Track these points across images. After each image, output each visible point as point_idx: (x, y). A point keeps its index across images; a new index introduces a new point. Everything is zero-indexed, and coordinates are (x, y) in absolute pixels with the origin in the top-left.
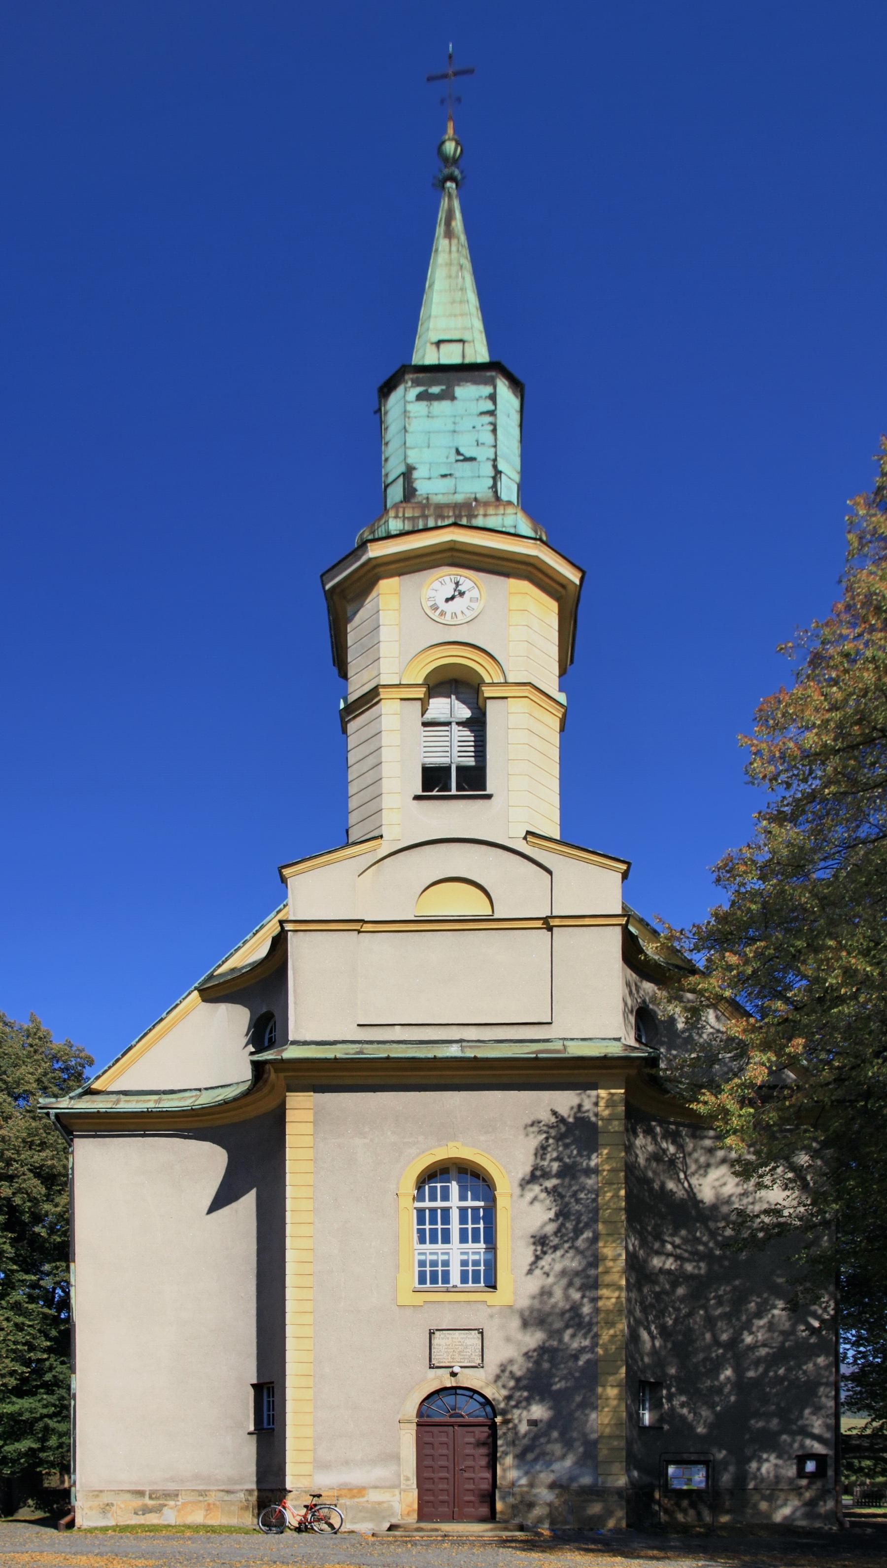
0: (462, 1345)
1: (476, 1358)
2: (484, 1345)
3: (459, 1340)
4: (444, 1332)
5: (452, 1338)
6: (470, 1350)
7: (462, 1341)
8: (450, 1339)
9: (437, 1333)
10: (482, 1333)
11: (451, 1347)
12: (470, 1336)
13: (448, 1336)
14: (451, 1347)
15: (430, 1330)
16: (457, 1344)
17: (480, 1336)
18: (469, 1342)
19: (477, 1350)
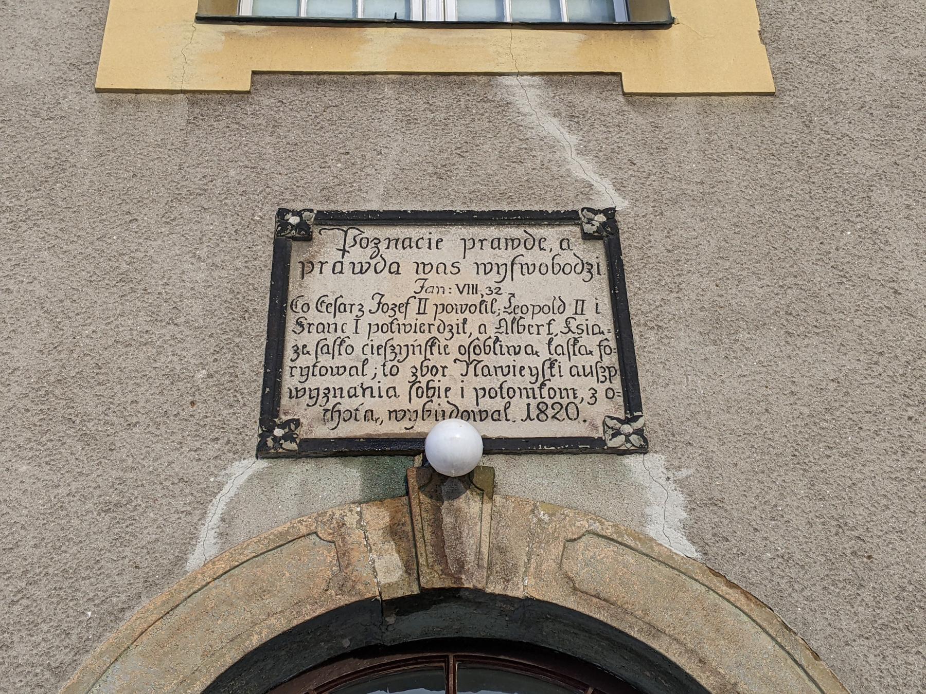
2: (634, 305)
3: (469, 275)
5: (421, 267)
6: (539, 342)
7: (486, 282)
8: (408, 269)
11: (412, 316)
13: (391, 255)
14: (412, 316)
16: (455, 298)
19: (590, 341)
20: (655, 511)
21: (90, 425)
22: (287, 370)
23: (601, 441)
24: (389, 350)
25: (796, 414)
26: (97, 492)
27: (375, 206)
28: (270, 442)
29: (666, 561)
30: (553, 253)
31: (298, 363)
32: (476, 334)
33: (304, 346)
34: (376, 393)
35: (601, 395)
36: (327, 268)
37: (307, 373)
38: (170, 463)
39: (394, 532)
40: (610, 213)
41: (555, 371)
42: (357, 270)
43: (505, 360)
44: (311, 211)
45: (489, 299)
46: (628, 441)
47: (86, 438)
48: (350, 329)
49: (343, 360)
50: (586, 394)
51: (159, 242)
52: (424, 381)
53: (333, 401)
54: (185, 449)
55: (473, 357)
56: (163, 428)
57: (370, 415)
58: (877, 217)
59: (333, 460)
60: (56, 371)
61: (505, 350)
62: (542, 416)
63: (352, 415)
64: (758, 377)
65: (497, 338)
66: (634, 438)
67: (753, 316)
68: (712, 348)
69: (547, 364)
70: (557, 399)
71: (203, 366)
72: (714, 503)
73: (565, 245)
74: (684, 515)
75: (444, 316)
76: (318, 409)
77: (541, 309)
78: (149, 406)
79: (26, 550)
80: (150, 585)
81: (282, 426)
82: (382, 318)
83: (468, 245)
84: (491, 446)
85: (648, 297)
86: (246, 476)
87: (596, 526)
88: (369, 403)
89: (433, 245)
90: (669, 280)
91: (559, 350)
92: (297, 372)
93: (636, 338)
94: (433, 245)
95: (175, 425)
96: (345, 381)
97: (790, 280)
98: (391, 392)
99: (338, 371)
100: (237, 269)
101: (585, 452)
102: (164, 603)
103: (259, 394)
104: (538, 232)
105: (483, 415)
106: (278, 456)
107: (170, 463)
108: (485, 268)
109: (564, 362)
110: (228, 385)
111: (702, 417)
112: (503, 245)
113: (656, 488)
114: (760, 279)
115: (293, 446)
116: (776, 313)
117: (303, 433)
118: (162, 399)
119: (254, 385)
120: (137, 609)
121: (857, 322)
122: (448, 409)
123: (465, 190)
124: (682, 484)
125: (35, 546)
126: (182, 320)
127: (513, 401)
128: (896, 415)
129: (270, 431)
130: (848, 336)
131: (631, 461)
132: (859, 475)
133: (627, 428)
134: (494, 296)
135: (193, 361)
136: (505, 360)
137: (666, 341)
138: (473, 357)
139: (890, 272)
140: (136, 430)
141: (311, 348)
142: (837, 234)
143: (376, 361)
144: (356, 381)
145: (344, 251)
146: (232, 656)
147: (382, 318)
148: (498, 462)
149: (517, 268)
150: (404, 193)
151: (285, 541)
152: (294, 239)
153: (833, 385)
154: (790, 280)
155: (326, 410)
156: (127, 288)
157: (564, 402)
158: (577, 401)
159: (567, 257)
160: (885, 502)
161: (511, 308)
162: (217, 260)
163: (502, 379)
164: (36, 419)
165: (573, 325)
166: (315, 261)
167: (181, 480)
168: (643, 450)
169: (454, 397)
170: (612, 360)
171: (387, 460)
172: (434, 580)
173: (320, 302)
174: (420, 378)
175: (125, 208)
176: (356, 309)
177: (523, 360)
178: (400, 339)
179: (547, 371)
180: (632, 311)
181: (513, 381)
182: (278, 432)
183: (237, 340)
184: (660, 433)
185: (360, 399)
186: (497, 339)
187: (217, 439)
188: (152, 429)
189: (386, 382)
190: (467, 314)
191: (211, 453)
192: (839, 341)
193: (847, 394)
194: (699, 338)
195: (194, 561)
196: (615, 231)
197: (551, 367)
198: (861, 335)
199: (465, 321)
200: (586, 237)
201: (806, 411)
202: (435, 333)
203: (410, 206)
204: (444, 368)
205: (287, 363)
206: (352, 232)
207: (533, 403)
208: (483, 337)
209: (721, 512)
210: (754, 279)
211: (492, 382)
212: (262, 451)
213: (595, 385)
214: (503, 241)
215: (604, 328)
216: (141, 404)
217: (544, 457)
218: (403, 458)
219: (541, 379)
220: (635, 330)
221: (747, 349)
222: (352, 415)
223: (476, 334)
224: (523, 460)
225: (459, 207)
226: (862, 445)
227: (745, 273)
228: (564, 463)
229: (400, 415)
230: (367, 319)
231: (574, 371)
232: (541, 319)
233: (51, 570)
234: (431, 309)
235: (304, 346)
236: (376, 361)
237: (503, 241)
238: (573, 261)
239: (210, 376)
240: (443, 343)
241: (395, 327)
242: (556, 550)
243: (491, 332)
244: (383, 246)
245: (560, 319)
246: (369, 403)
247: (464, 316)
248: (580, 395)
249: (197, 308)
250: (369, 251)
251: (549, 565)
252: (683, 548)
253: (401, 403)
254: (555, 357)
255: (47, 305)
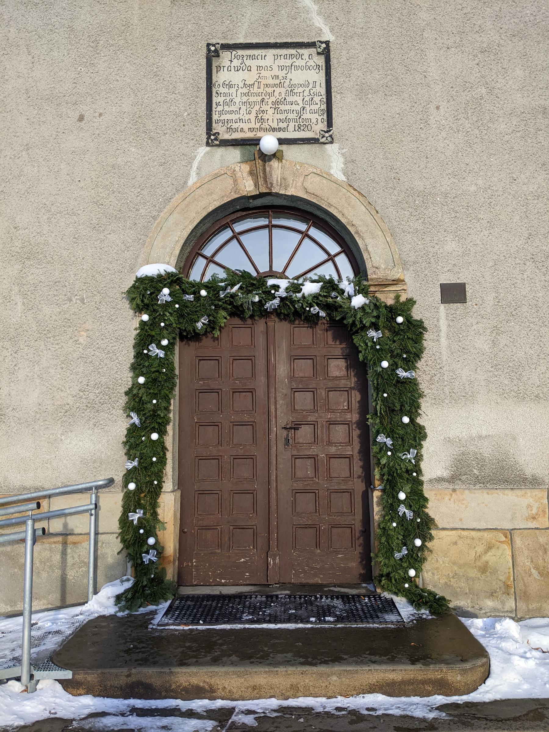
0: (280, 85)
1: (314, 117)
3: (276, 72)
4: (240, 52)
5: (259, 67)
6: (299, 99)
7: (282, 74)
8: (254, 69)
9: (226, 55)
10: (326, 53)
11: (255, 90)
12: (299, 62)
13: (248, 62)
14: (255, 90)
15: (208, 45)
16: (270, 81)
17: (321, 60)
18: (297, 77)
19: (317, 99)
20: (334, 165)
21: (152, 134)
22: (214, 112)
23: (318, 139)
24: (248, 104)
25: (384, 127)
26: (157, 159)
27: (241, 40)
28: (210, 141)
29: (336, 182)
30: (306, 61)
31: (217, 109)
32: (278, 97)
33: (219, 102)
34: (244, 121)
35: (319, 121)
36: (226, 69)
37: (221, 113)
38: (179, 148)
39: (251, 173)
40: (327, 43)
41: (305, 111)
42: (236, 69)
43: (287, 107)
44: (218, 44)
45: (282, 81)
46: (327, 139)
47: (151, 138)
48: (234, 95)
49: (233, 108)
50: (314, 121)
51: (166, 59)
52: (260, 116)
53: (230, 124)
54: (183, 143)
55: (277, 106)
56: (175, 135)
57: (242, 130)
58: (424, 44)
59: (231, 147)
60: (138, 113)
61: (288, 103)
62: (299, 130)
63: (236, 130)
64: (373, 113)
65: (285, 98)
66: (329, 138)
67: (374, 88)
68: (358, 101)
69: (302, 109)
70: (305, 123)
71: (186, 110)
72: (353, 161)
73: (310, 57)
74: (343, 166)
75: (267, 89)
76: (225, 128)
77: (301, 86)
78: (170, 127)
79: (138, 179)
80: (178, 191)
81: (214, 135)
82: (245, 90)
83: (276, 57)
84: (281, 141)
85: (339, 80)
86: (203, 153)
87: (315, 171)
88: (242, 125)
89: (263, 58)
90: (346, 72)
91: (306, 103)
92: (217, 113)
93: (333, 97)
94: (263, 58)
95: (179, 134)
96: (234, 117)
97: (389, 72)
98: (249, 121)
99: (231, 112)
100: (194, 70)
101: (313, 143)
102: (183, 197)
103: (205, 122)
104: (301, 51)
105: (280, 129)
106: (213, 146)
107: (179, 148)
108: (281, 68)
109: (308, 108)
110: (195, 118)
111: (352, 129)
112: (288, 57)
113: (335, 157)
114: (379, 72)
115: (218, 143)
116: (382, 86)
117: (220, 137)
118: (174, 124)
119: (203, 118)
120: (175, 198)
121: (410, 90)
122: (268, 127)
123: (275, 32)
124: (343, 154)
125: (141, 177)
126: (177, 92)
127: (290, 124)
128: (417, 127)
129: (210, 137)
130: (406, 95)
131: (328, 146)
132: (400, 150)
133: (327, 135)
134: (284, 80)
135: (182, 109)
136: (287, 107)
137: (343, 99)
138: (277, 106)
139: (424, 68)
140: (167, 136)
141: (221, 103)
142: (408, 51)
143: (244, 108)
144: (237, 116)
145: (231, 61)
146: (204, 214)
147: (245, 90)
148: (284, 147)
149: (293, 67)
150: (252, 34)
151: (217, 176)
152: (213, 56)
153: (398, 116)
154: (389, 72)
155: (228, 128)
156: (157, 78)
157: (307, 124)
158: (311, 124)
159: (311, 63)
160: (407, 160)
161: (291, 86)
162: (187, 66)
163: (286, 115)
164: (134, 131)
165: (312, 92)
166: (221, 66)
167: (183, 154)
168: (332, 142)
169: (270, 122)
170: (324, 107)
171: (248, 147)
172: (264, 190)
173: (224, 84)
174: (259, 115)
175: (153, 44)
176: (236, 86)
177: (294, 107)
178: (252, 99)
179: (302, 112)
180: (332, 86)
181: (291, 116)
182: (212, 137)
183: (196, 100)
184: (338, 135)
185: (239, 124)
186: (285, 98)
187: (193, 139)
188: (172, 135)
189: (247, 117)
190: (275, 88)
191: (192, 145)
192: (402, 97)
193: (402, 119)
194: (355, 97)
195: (190, 183)
196: (329, 51)
197: (303, 110)
198: (410, 95)
199: (274, 91)
200: (319, 54)
201: (387, 126)
202: (264, 97)
203: (255, 41)
204: (267, 111)
205: (214, 109)
206: (234, 53)
207: (297, 124)
208: (280, 98)
209: (355, 165)
210: (376, 71)
211: (282, 116)
212: (208, 144)
213: (318, 117)
214: (288, 55)
215: (322, 94)
216: (167, 126)
217: (299, 145)
218: (253, 146)
219: (299, 115)
220: (333, 94)
221: (371, 101)
222: (236, 130)
223: (278, 97)
224: (292, 146)
225: (272, 41)
226: (403, 139)
227: (373, 69)
228: (306, 148)
229: (252, 130)
230: (240, 91)
231: (311, 112)
232: (301, 90)
233: (147, 185)
234: (262, 86)
235: (219, 102)
236: (244, 108)
237: (288, 55)
238: (313, 64)
239: (189, 115)
240: (266, 100)
241: (250, 94)
242: (301, 179)
243: (283, 96)
244: (245, 58)
245: (307, 90)
246: (242, 125)
247: (273, 89)
248: (312, 121)
249: (182, 87)
250: (240, 61)
251: (299, 184)
252: (341, 177)
253: (252, 125)
254: (305, 106)
255: (131, 86)
